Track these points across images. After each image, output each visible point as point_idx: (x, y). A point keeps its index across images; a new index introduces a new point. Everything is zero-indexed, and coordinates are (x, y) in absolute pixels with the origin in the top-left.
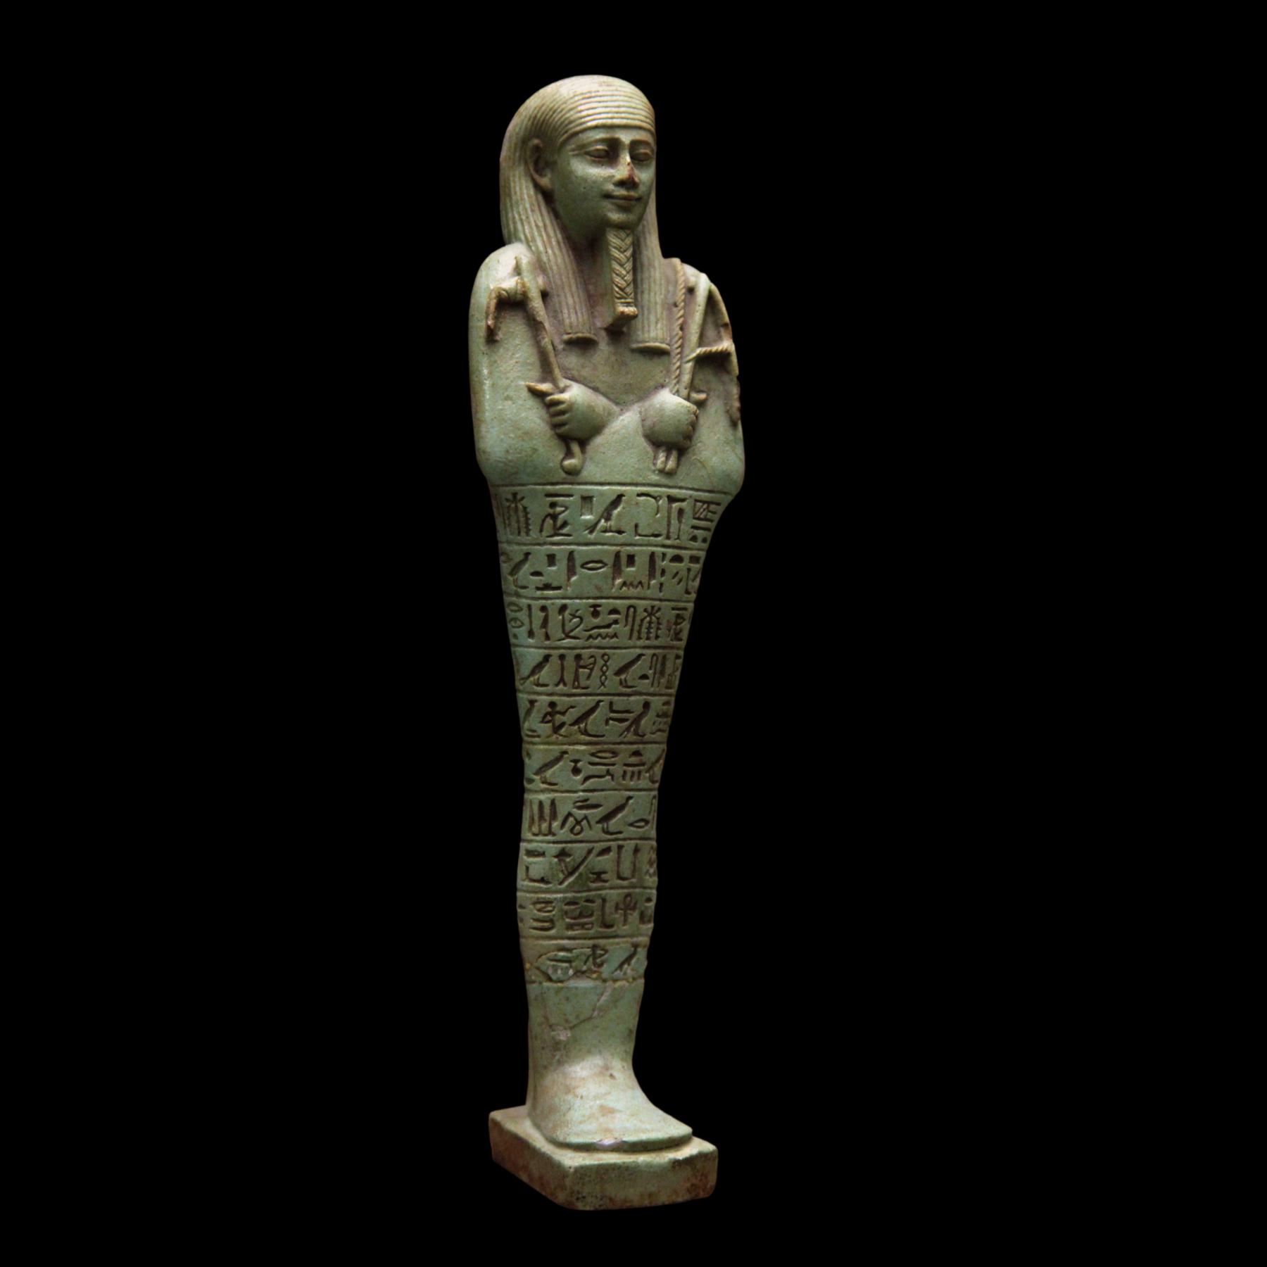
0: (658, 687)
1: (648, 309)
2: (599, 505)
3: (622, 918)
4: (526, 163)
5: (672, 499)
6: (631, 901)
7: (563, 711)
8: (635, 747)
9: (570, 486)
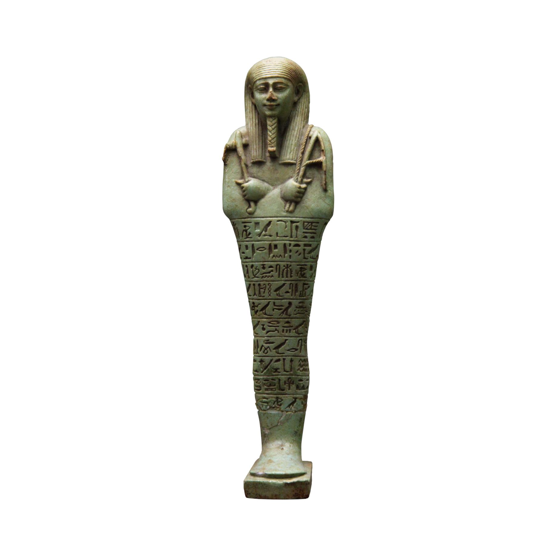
0: (295, 296)
1: (288, 147)
2: (262, 226)
3: (288, 387)
4: (249, 95)
5: (292, 222)
6: (291, 380)
7: (257, 305)
8: (287, 320)
9: (251, 219)
